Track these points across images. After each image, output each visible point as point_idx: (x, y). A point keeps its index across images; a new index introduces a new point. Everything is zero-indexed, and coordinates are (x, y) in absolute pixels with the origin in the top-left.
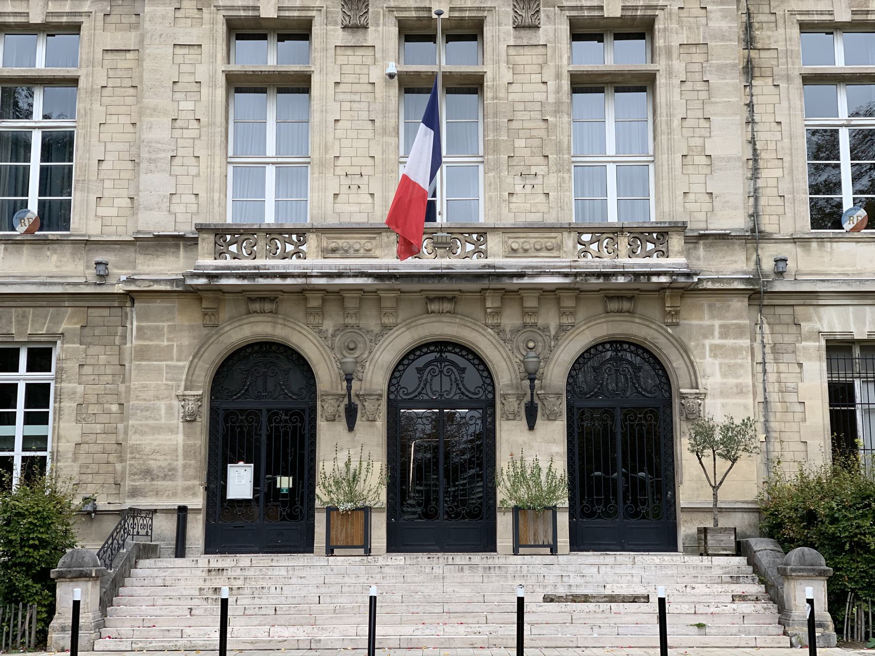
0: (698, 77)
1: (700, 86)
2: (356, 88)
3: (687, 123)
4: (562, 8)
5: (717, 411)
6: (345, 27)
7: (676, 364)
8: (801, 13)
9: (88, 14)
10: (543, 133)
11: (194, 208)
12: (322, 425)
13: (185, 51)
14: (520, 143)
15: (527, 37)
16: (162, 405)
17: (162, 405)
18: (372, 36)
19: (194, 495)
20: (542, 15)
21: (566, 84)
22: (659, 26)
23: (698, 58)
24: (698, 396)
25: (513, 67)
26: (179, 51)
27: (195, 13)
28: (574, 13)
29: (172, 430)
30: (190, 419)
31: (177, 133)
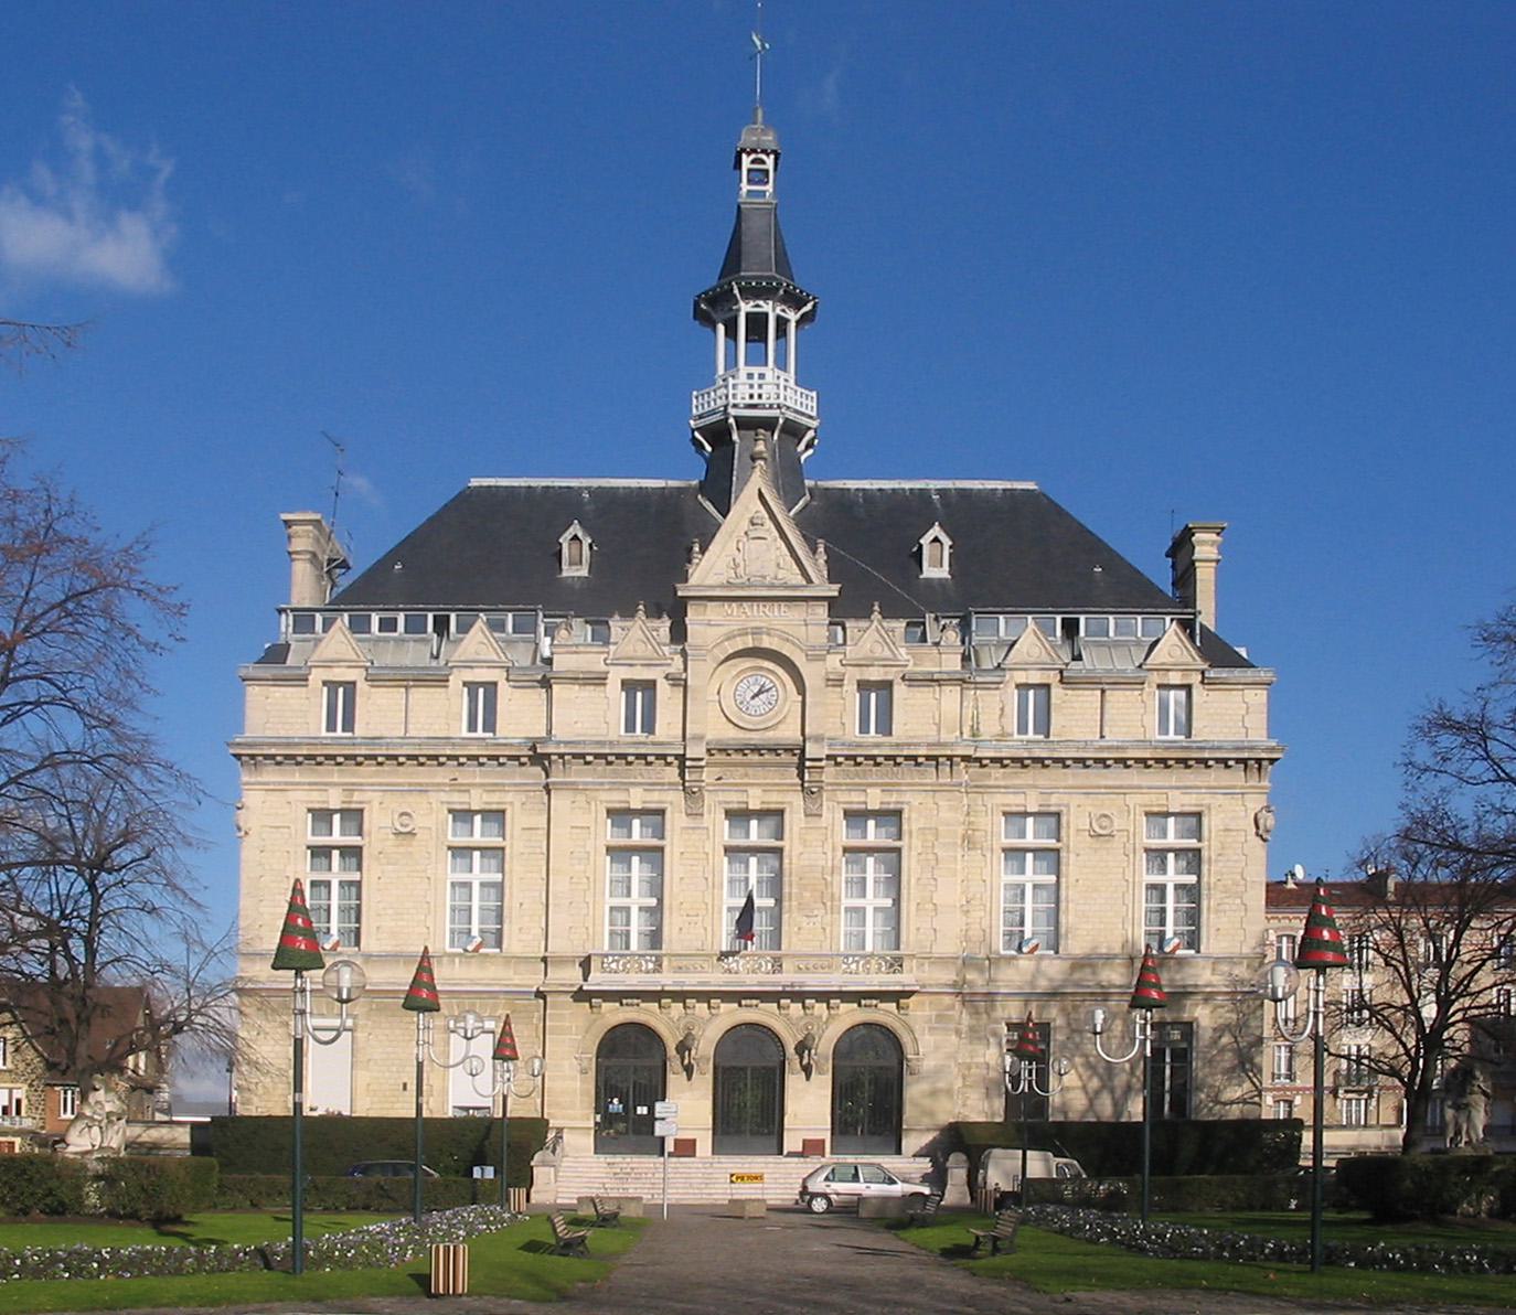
0: (929, 850)
1: (931, 857)
2: (696, 856)
3: (921, 882)
4: (838, 803)
5: (928, 1064)
6: (688, 815)
7: (906, 1039)
8: (1004, 805)
9: (511, 803)
10: (823, 887)
11: (585, 937)
12: (670, 1077)
13: (579, 831)
14: (807, 894)
15: (813, 822)
16: (566, 1063)
17: (566, 1063)
18: (707, 820)
19: (588, 1119)
20: (825, 807)
21: (840, 852)
22: (905, 815)
23: (930, 838)
24: (918, 1060)
25: (804, 843)
26: (574, 831)
27: (584, 805)
28: (846, 806)
29: (573, 1079)
30: (584, 1072)
31: (573, 886)
